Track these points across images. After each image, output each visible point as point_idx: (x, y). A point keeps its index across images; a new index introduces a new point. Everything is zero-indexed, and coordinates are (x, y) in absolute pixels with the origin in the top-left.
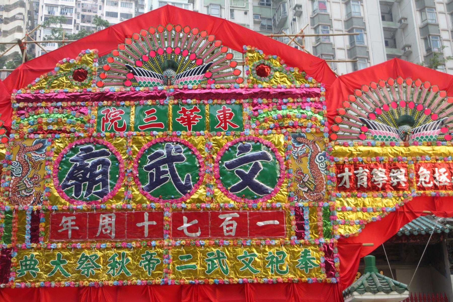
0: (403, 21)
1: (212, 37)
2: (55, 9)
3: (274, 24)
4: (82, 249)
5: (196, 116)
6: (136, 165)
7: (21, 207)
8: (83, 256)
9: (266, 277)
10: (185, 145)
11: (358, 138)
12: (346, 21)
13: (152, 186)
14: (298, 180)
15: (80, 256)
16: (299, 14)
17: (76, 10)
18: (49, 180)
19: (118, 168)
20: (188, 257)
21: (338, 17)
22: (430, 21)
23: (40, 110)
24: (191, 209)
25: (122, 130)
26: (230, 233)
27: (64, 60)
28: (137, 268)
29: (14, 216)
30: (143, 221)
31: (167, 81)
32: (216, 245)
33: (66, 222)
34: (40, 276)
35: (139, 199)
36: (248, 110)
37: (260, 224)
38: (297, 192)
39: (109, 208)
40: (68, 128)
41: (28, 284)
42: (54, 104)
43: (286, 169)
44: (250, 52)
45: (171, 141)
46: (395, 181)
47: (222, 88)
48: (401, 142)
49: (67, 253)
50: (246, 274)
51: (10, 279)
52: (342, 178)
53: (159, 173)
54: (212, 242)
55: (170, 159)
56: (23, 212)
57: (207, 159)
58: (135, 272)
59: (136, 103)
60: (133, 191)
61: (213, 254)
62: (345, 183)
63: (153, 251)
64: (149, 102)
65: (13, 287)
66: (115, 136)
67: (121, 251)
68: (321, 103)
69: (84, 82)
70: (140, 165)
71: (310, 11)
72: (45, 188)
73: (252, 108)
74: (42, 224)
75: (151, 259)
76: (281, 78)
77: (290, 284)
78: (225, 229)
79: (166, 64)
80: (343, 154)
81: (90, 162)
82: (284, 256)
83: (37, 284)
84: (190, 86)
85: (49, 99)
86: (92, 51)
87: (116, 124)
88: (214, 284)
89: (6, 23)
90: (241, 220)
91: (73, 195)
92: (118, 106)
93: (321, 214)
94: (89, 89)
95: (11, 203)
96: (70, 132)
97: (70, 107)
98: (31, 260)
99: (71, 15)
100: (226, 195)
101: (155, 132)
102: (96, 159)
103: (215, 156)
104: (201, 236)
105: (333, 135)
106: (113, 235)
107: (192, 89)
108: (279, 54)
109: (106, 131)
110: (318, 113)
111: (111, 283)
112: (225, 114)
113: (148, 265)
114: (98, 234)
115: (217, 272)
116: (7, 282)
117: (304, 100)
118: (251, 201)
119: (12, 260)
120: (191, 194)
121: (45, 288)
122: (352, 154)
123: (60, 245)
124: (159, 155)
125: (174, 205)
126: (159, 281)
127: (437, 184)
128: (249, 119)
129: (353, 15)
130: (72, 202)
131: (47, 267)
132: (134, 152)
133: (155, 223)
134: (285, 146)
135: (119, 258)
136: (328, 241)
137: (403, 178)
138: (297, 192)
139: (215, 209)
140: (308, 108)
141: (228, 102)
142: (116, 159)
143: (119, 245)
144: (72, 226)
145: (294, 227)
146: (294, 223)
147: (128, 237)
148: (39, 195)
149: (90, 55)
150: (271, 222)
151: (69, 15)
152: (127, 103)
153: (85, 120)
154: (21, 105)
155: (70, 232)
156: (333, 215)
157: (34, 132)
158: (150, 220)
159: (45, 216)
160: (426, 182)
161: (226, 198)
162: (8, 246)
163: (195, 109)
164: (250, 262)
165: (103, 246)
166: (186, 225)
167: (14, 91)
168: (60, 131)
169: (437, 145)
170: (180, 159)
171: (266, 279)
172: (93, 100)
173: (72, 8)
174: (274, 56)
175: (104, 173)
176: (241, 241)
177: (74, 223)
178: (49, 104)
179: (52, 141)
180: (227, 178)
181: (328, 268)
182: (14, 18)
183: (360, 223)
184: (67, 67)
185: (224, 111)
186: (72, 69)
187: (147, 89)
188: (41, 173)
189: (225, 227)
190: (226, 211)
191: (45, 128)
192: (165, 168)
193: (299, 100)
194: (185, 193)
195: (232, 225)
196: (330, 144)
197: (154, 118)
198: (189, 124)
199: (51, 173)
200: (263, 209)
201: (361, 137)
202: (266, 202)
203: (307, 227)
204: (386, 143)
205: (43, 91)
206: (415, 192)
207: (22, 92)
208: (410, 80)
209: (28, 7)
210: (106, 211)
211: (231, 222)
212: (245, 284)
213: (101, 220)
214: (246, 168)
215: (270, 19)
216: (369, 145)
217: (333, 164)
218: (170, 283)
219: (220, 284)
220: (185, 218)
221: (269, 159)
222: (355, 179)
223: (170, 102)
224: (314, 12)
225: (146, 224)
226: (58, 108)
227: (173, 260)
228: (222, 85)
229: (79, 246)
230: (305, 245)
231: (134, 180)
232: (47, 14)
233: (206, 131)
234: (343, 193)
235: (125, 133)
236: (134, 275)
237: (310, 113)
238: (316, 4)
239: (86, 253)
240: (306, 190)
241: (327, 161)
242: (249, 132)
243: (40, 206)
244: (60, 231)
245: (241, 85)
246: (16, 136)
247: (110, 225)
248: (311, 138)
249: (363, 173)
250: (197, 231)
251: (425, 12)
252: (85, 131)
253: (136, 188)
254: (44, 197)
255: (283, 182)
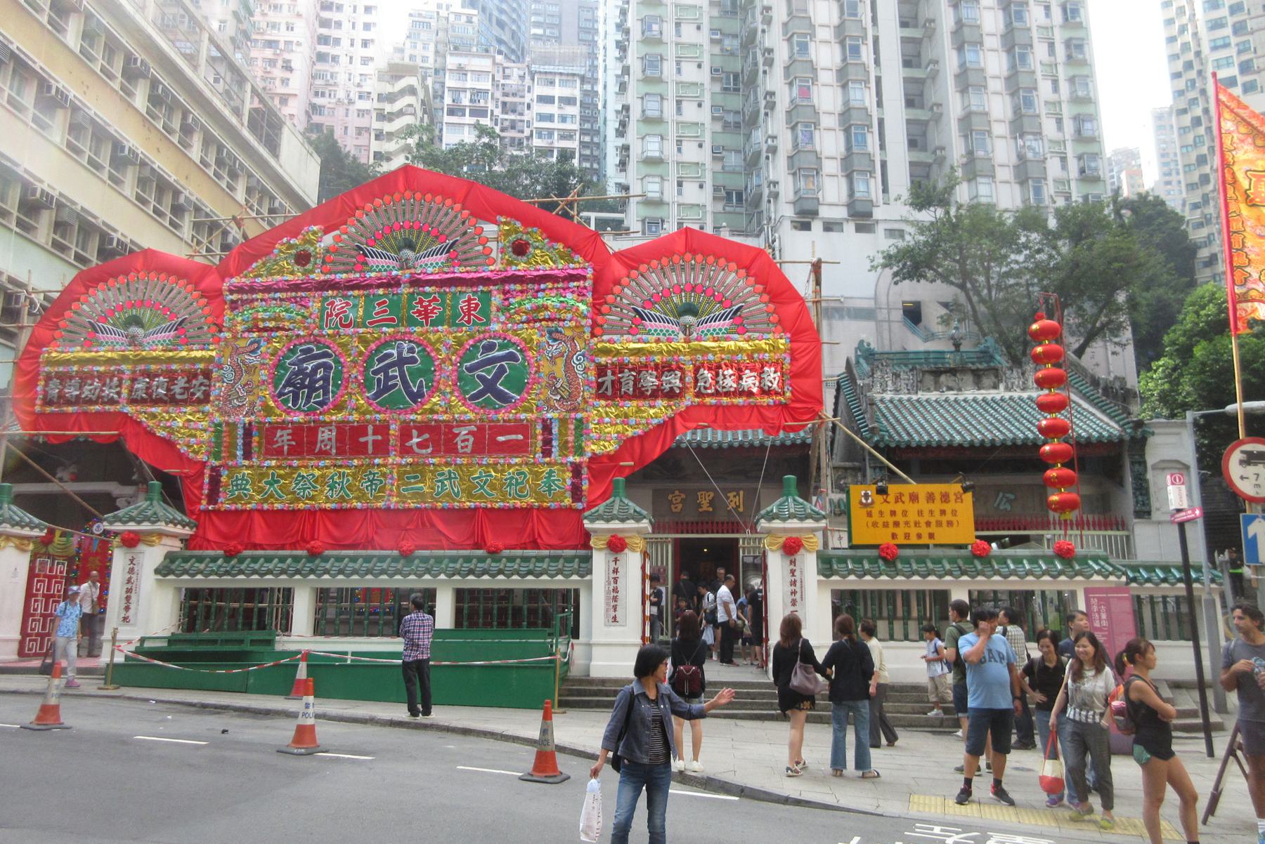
0: (935, 108)
1: (458, 206)
2: (462, 95)
3: (744, 121)
4: (299, 467)
5: (434, 308)
6: (362, 369)
7: (232, 420)
8: (299, 475)
9: (503, 501)
10: (419, 345)
11: (629, 333)
12: (840, 115)
13: (377, 396)
14: (549, 386)
15: (295, 476)
16: (771, 106)
17: (492, 94)
18: (263, 387)
19: (341, 372)
20: (415, 477)
21: (830, 109)
22: (974, 108)
23: (256, 303)
24: (423, 422)
25: (348, 326)
26: (466, 450)
27: (285, 240)
28: (359, 489)
29: (225, 429)
30: (366, 435)
31: (404, 265)
32: (447, 464)
33: (282, 436)
34: (252, 497)
35: (363, 409)
36: (497, 299)
37: (501, 439)
38: (547, 401)
39: (328, 420)
40: (287, 324)
41: (239, 506)
42: (272, 295)
43: (536, 372)
44: (505, 223)
45: (404, 340)
46: (667, 387)
47: (467, 272)
48: (681, 335)
49: (282, 472)
50: (481, 496)
51: (220, 500)
52: (603, 383)
53: (387, 378)
54: (444, 460)
55: (401, 362)
56: (235, 425)
57: (443, 361)
58: (356, 494)
59: (366, 292)
60: (357, 400)
61: (443, 474)
62: (606, 390)
63: (375, 470)
64: (381, 291)
65: (223, 509)
66: (338, 333)
67: (342, 470)
68: (585, 288)
69: (307, 267)
70: (366, 369)
71: (787, 100)
72: (259, 397)
73: (502, 296)
74: (256, 439)
75: (373, 479)
76: (542, 256)
77: (529, 510)
78: (460, 445)
79: (402, 244)
80: (606, 352)
81: (309, 366)
82: (525, 477)
83: (249, 507)
84: (430, 270)
85: (268, 289)
86: (315, 228)
87: (341, 319)
88: (443, 509)
89: (390, 120)
90: (479, 434)
91: (290, 405)
92: (345, 296)
93: (572, 427)
94: (312, 276)
95: (222, 415)
96: (290, 329)
97: (289, 299)
98: (243, 479)
99: (486, 102)
100: (463, 404)
101: (384, 329)
102: (316, 362)
103: (454, 358)
104: (432, 452)
105: (597, 330)
106: (334, 451)
107: (432, 274)
108: (539, 226)
109: (330, 328)
110: (582, 301)
111: (328, 505)
112: (469, 305)
113: (371, 486)
114: (317, 450)
115: (448, 495)
116: (216, 503)
117: (565, 286)
118: (493, 412)
119: (222, 479)
120: (423, 404)
121: (258, 510)
122: (618, 352)
123: (273, 463)
124: (390, 355)
125: (402, 417)
126: (381, 504)
127: (720, 389)
128: (498, 311)
129: (852, 104)
130: (288, 413)
131: (259, 487)
132: (361, 353)
133: (379, 438)
134: (539, 344)
135: (339, 478)
136: (578, 459)
137: (677, 382)
138: (547, 401)
139: (449, 421)
140: (569, 296)
141: (475, 289)
142: (340, 362)
143: (339, 463)
144: (288, 440)
145: (540, 444)
146: (540, 437)
147: (351, 454)
148: (252, 404)
149: (314, 233)
150: (513, 437)
151: (482, 103)
152: (356, 293)
153: (306, 314)
154: (235, 297)
155: (286, 448)
156: (587, 428)
157: (249, 330)
158: (375, 433)
159: (258, 429)
160: (706, 388)
161: (463, 408)
162: (217, 463)
163: (435, 299)
164: (485, 483)
165: (321, 464)
166: (416, 440)
167: (227, 280)
168: (278, 329)
169: (727, 339)
170: (413, 360)
171: (502, 504)
172: (317, 289)
173: (486, 92)
174: (535, 229)
175: (325, 379)
176: (475, 460)
177: (290, 437)
178: (267, 296)
179: (269, 341)
180: (466, 385)
181: (576, 492)
182: (401, 113)
183: (617, 438)
184: (288, 249)
185: (469, 300)
186: (293, 251)
187: (379, 275)
188: (256, 379)
189: (459, 443)
190: (462, 424)
191: (261, 325)
192: (394, 372)
193: (560, 285)
194: (415, 402)
195: (467, 440)
196: (592, 341)
197: (385, 311)
198: (426, 318)
199: (265, 378)
200: (504, 421)
201: (631, 331)
202: (510, 412)
203: (555, 443)
204: (661, 337)
205: (259, 280)
206: (689, 399)
207: (235, 280)
208: (643, 267)
209: (421, 94)
210: (325, 424)
211: (467, 437)
212: (477, 509)
213: (320, 435)
214: (489, 372)
215: (737, 112)
216: (639, 341)
217: (592, 366)
218: (392, 507)
219: (449, 509)
220: (415, 433)
221: (518, 360)
222: (616, 384)
223: (405, 290)
224: (792, 101)
225: (370, 438)
226: (275, 299)
227: (399, 480)
228: (468, 268)
229: (296, 463)
230: (549, 464)
231: (359, 386)
232: (451, 103)
233: (446, 327)
234: (603, 402)
235: (351, 330)
236: (354, 498)
237: (572, 302)
238: (795, 90)
239: (303, 472)
240: (558, 397)
241: (586, 363)
242: (496, 327)
243: (253, 417)
244: (275, 446)
245: (492, 268)
246: (228, 335)
247: (330, 440)
248: (569, 333)
249: (627, 377)
250: (427, 447)
251: (968, 92)
252: (305, 328)
253: (361, 396)
254: (258, 408)
255: (532, 389)
